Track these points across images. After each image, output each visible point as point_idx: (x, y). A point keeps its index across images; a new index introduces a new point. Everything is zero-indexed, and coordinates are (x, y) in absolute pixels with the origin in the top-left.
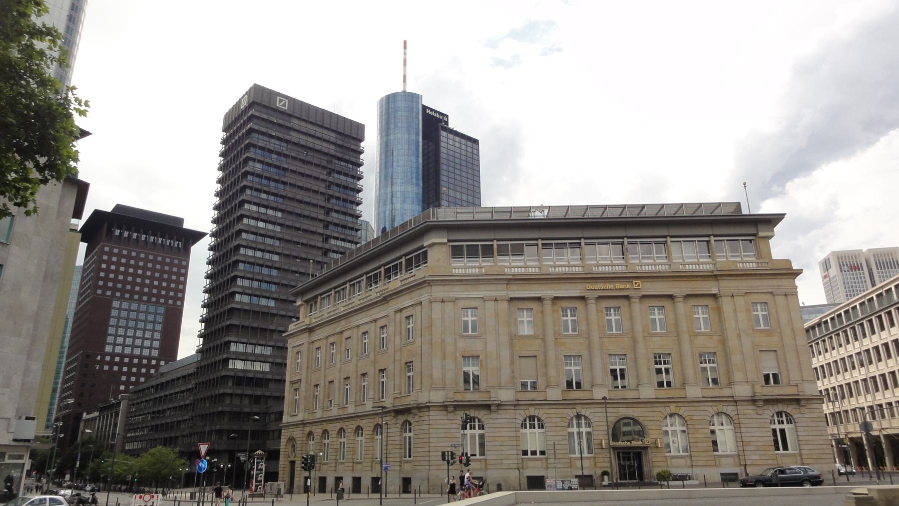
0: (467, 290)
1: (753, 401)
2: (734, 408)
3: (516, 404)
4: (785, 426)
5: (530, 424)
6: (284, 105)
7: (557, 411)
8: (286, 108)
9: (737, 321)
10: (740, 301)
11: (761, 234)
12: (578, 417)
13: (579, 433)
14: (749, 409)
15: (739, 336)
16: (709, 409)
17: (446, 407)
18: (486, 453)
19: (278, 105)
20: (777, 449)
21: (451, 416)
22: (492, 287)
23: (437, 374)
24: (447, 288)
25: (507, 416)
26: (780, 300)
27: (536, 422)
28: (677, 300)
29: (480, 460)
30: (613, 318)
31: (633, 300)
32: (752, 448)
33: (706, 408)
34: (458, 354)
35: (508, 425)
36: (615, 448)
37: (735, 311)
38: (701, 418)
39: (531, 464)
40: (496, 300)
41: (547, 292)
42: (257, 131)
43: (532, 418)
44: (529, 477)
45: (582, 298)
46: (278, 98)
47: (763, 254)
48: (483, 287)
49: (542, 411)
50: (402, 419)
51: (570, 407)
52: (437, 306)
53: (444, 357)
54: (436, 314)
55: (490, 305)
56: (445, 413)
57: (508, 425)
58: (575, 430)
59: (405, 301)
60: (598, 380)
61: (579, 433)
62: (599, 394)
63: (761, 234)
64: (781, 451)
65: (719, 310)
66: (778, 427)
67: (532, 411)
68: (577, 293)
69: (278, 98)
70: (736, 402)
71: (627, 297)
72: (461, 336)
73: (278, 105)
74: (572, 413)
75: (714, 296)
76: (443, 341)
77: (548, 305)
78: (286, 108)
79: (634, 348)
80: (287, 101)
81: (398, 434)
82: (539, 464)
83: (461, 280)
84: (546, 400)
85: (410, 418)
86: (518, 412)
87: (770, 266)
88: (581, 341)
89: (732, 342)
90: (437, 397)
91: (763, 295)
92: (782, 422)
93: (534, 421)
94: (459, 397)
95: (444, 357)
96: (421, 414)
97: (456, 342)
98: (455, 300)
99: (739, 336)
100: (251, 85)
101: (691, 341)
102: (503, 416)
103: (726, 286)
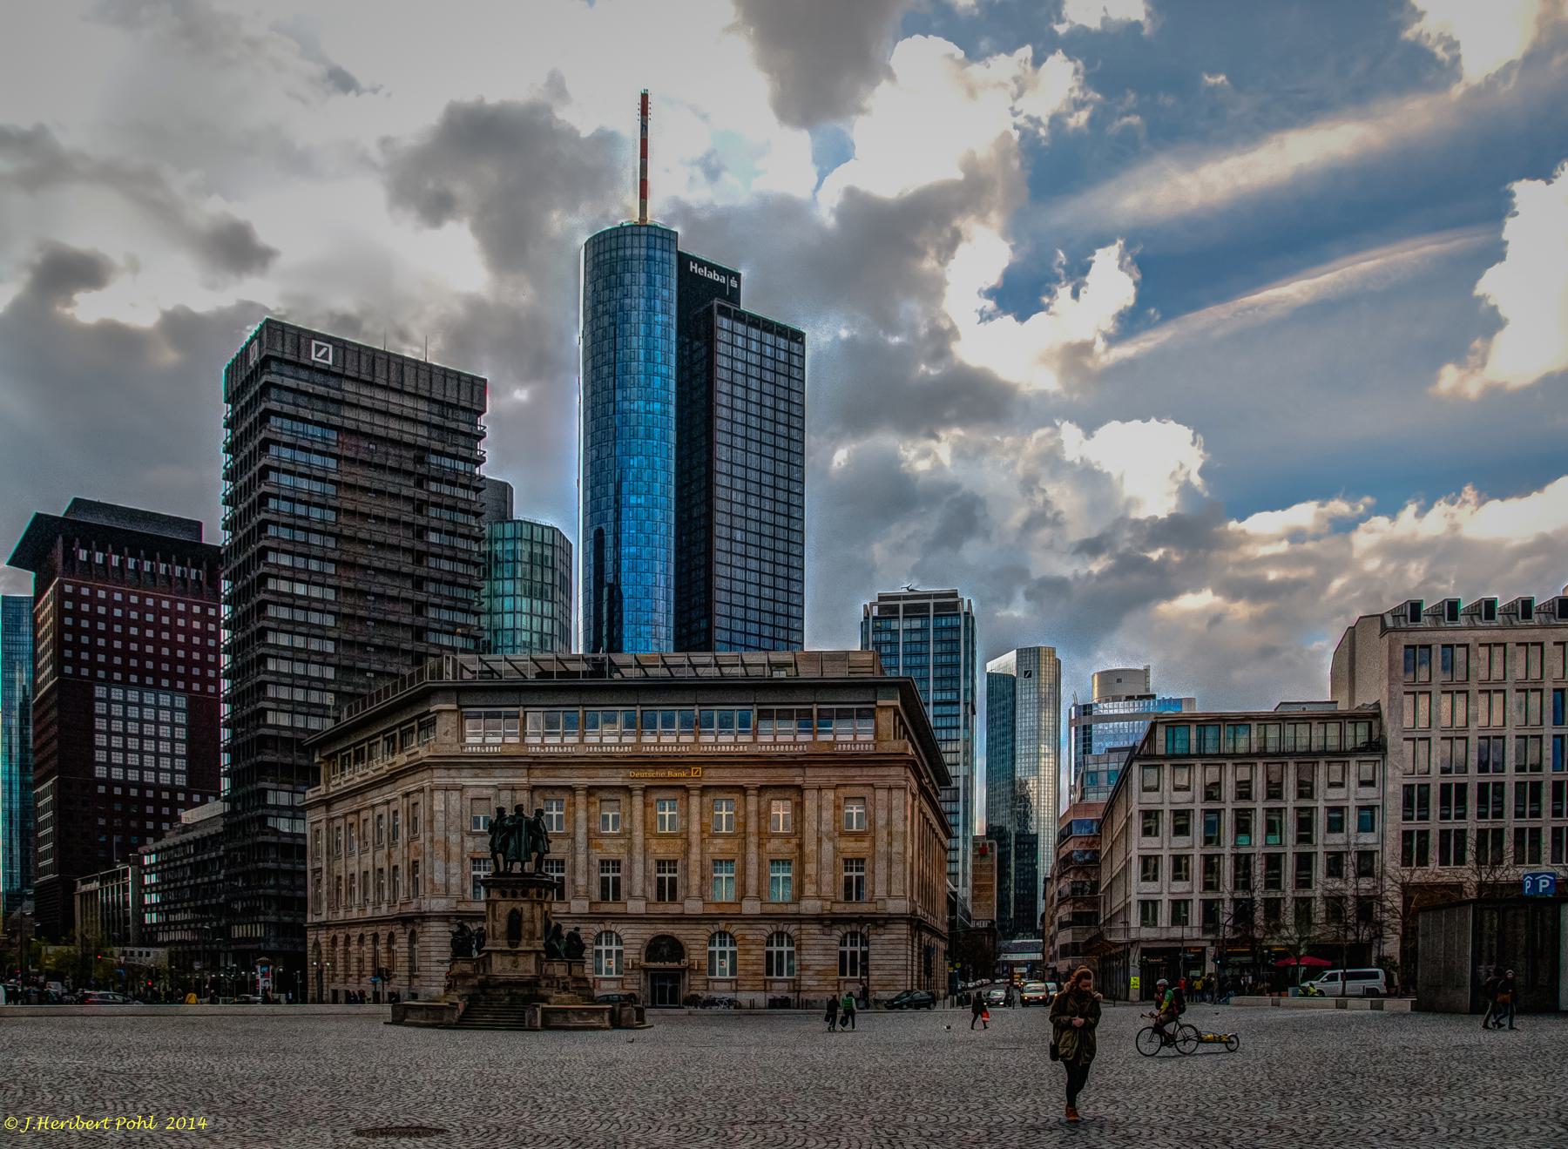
0: (476, 776)
6: (325, 357)
8: (330, 362)
9: (819, 823)
10: (830, 795)
13: (780, 954)
14: (814, 929)
15: (819, 840)
17: (448, 917)
19: (313, 358)
20: (843, 973)
22: (510, 772)
23: (439, 878)
24: (453, 773)
28: (749, 792)
30: (667, 813)
36: (646, 970)
37: (820, 807)
40: (513, 789)
41: (579, 779)
42: (279, 414)
45: (627, 790)
46: (314, 343)
48: (497, 772)
52: (439, 797)
53: (448, 859)
54: (439, 805)
58: (604, 948)
59: (410, 784)
60: (638, 892)
62: (636, 907)
64: (848, 976)
66: (848, 949)
68: (618, 781)
69: (314, 343)
70: (800, 919)
71: (686, 789)
72: (470, 834)
73: (313, 358)
76: (447, 839)
77: (581, 799)
78: (330, 362)
79: (686, 853)
80: (331, 347)
88: (622, 841)
89: (810, 847)
92: (854, 944)
95: (448, 859)
97: (462, 841)
98: (462, 789)
99: (819, 840)
101: (760, 845)
103: (812, 776)
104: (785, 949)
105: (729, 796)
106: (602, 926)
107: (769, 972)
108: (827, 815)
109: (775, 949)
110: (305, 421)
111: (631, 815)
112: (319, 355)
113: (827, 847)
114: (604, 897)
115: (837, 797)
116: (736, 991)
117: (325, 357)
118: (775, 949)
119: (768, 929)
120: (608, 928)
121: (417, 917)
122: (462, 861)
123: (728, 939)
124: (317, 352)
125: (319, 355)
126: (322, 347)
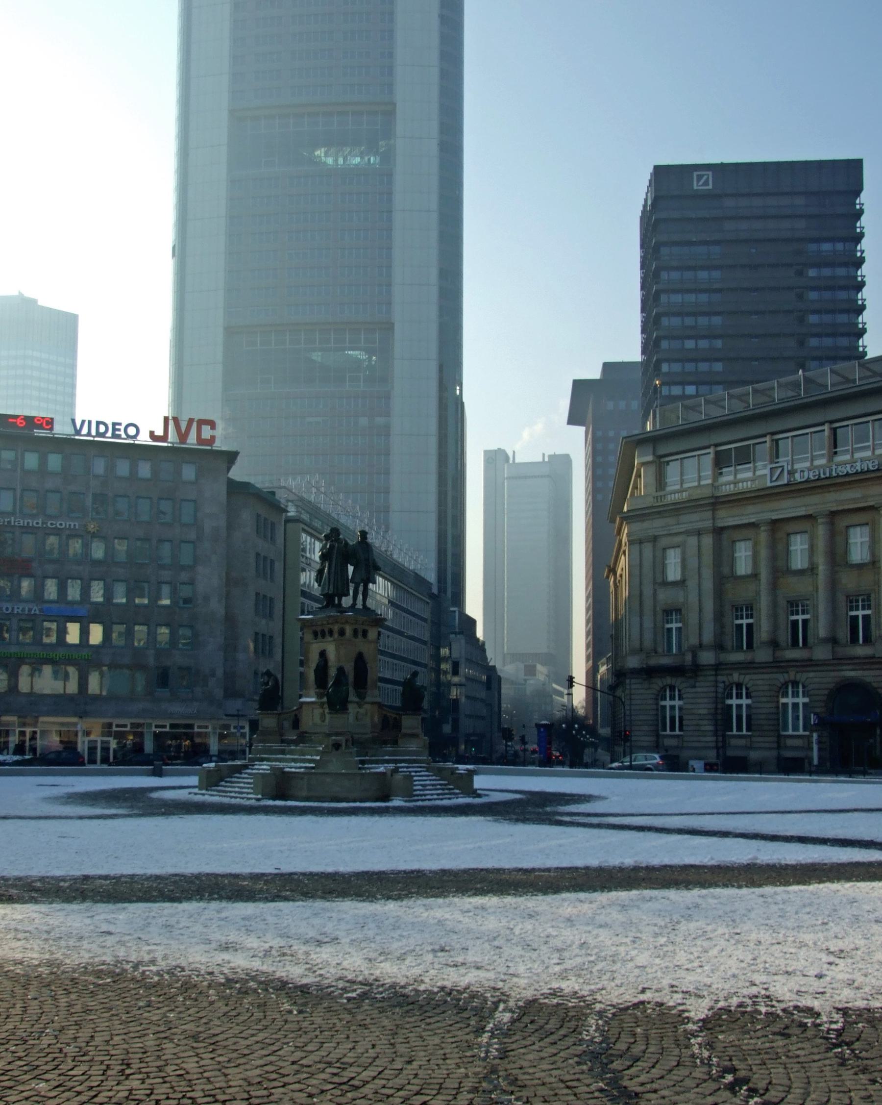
3: (718, 667)
5: (793, 692)
6: (706, 183)
7: (766, 676)
8: (710, 187)
12: (795, 684)
18: (685, 728)
19: (695, 187)
27: (801, 690)
29: (678, 736)
34: (658, 609)
39: (734, 742)
42: (665, 244)
43: (739, 686)
46: (695, 174)
49: (748, 677)
51: (782, 670)
55: (693, 541)
61: (795, 706)
67: (736, 677)
68: (801, 512)
73: (695, 187)
74: (782, 678)
78: (710, 187)
80: (710, 173)
83: (659, 512)
84: (812, 660)
93: (798, 687)
100: (651, 170)
106: (786, 675)
110: (691, 243)
112: (701, 183)
114: (854, 639)
117: (706, 183)
120: (792, 678)
122: (655, 615)
123: (801, 690)
124: (698, 181)
125: (701, 183)
126: (703, 175)
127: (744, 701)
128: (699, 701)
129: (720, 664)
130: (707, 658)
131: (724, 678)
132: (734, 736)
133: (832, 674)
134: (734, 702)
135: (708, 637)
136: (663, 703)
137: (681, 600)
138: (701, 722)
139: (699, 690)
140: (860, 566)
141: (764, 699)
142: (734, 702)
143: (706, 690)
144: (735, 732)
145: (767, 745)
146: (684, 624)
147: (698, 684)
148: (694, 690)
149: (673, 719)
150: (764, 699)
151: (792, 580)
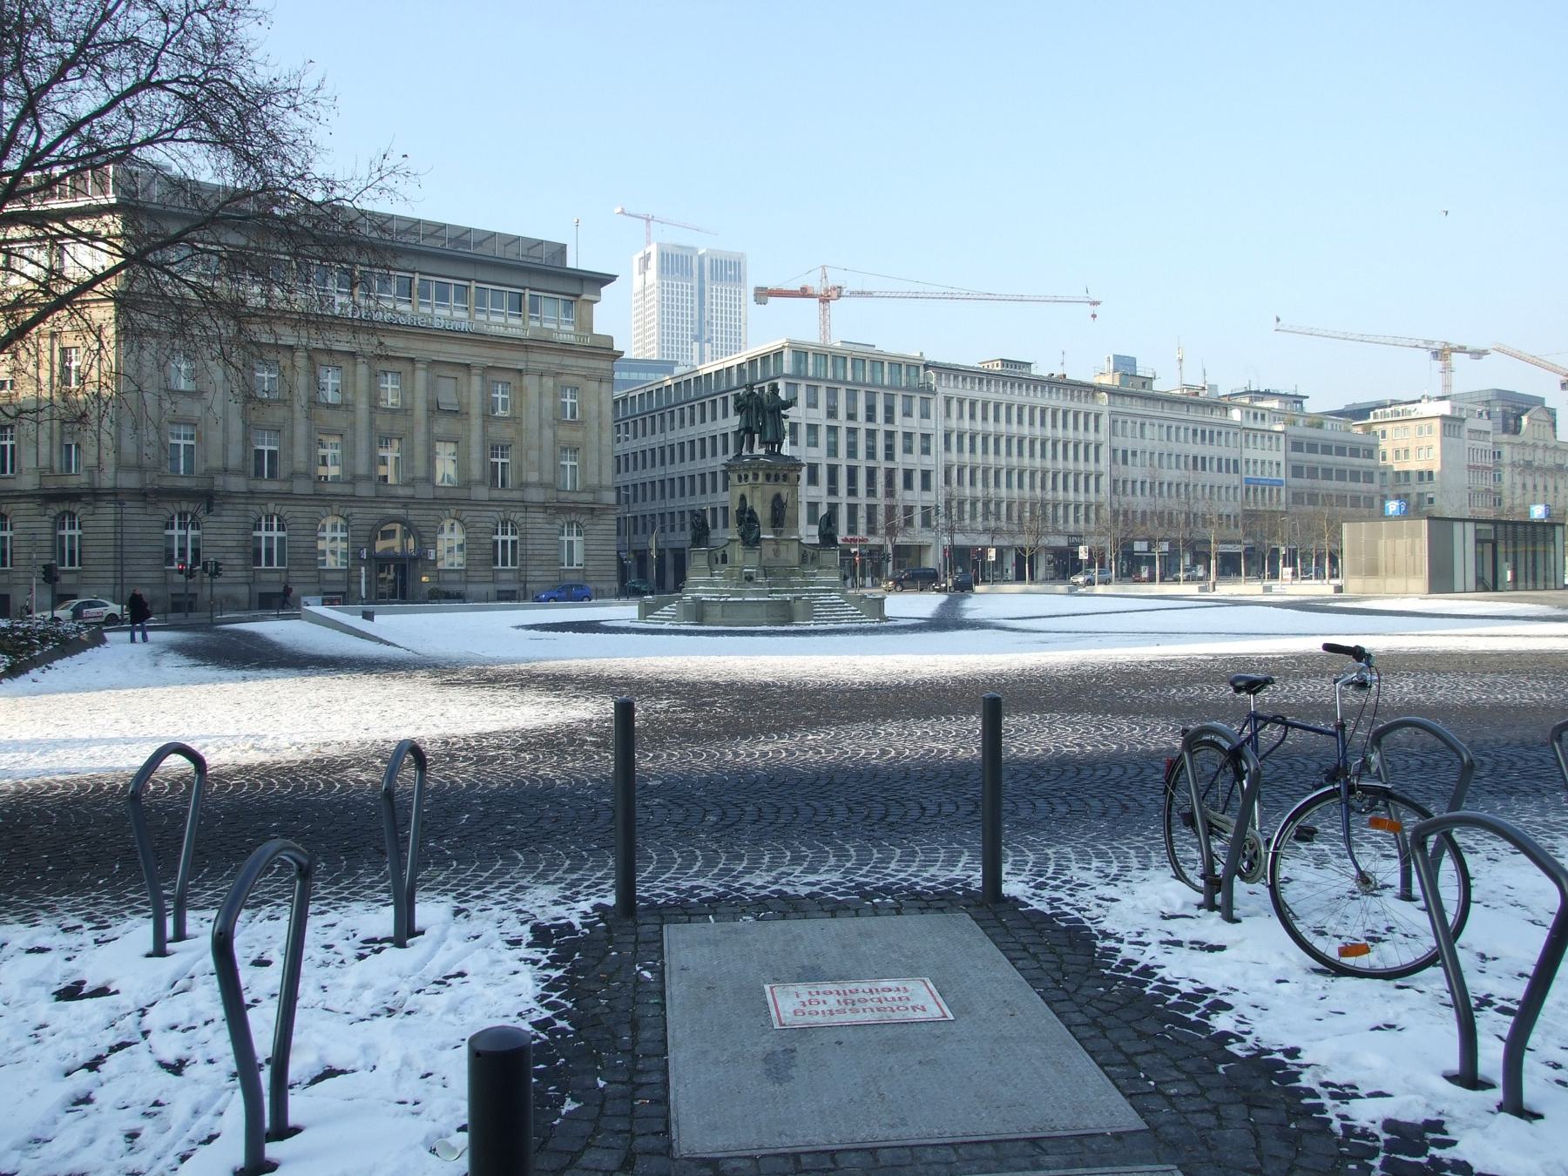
1: (544, 507)
2: (523, 515)
4: (575, 538)
7: (306, 509)
11: (585, 296)
14: (539, 518)
16: (495, 514)
17: (145, 495)
21: (150, 510)
25: (236, 513)
26: (594, 385)
28: (474, 371)
31: (419, 365)
32: (535, 563)
33: (490, 514)
35: (236, 525)
37: (540, 394)
38: (483, 525)
39: (264, 577)
44: (261, 594)
47: (586, 324)
50: (55, 509)
56: (140, 504)
57: (236, 525)
63: (585, 296)
65: (521, 390)
67: (271, 507)
70: (526, 506)
71: (412, 360)
75: (520, 371)
81: (49, 531)
82: (275, 577)
85: (76, 508)
86: (250, 507)
87: (588, 341)
90: (130, 481)
91: (575, 378)
94: (166, 483)
96: (99, 504)
102: (230, 513)
103: (539, 360)
104: (509, 538)
105: (453, 374)
107: (496, 563)
108: (548, 402)
109: (500, 538)
111: (354, 385)
113: (548, 433)
115: (555, 385)
116: (467, 582)
118: (500, 538)
119: (497, 515)
121: (87, 494)
127: (276, 534)
128: (228, 531)
129: (251, 492)
130: (237, 484)
131: (257, 508)
132: (265, 571)
133: (375, 511)
134: (263, 534)
135: (234, 460)
136: (62, 533)
137: (197, 413)
138: (228, 556)
139: (226, 519)
140: (393, 411)
141: (304, 532)
142: (263, 534)
143: (234, 519)
144: (263, 566)
145: (307, 580)
146: (199, 441)
147: (224, 513)
148: (218, 519)
149: (72, 553)
150: (304, 532)
151: (326, 413)
